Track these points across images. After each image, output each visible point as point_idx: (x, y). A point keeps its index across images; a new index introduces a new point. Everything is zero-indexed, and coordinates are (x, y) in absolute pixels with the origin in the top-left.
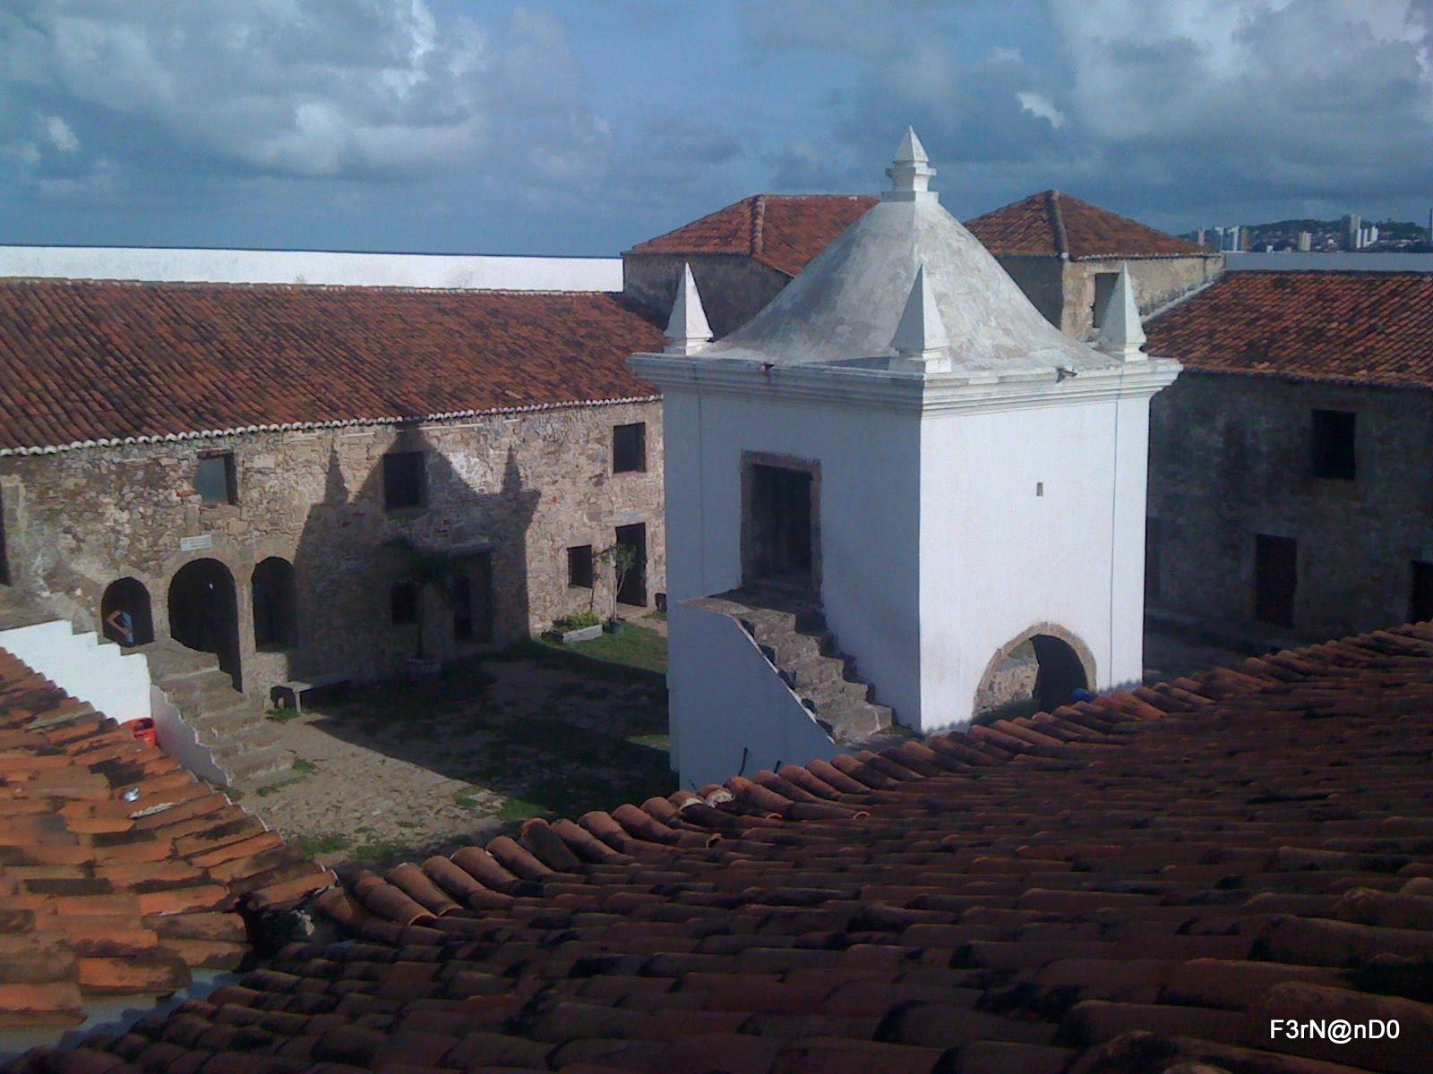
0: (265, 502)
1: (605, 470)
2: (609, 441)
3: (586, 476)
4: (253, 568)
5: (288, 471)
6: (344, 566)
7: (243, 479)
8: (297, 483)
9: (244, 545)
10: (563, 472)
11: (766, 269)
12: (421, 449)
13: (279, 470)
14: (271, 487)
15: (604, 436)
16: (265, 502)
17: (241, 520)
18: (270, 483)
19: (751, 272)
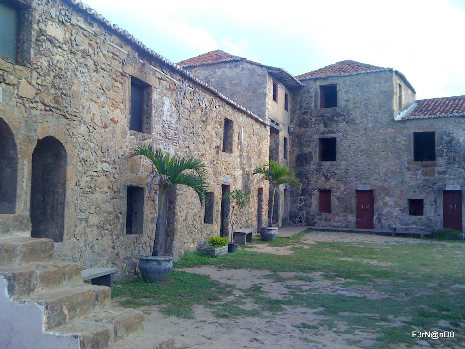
0: (52, 74)
1: (220, 145)
2: (223, 126)
3: (214, 145)
4: (35, 143)
5: (71, 53)
6: (101, 166)
7: (37, 40)
8: (77, 69)
9: (30, 114)
10: (207, 137)
11: (253, 66)
12: (151, 84)
13: (65, 47)
14: (58, 61)
15: (222, 122)
16: (52, 74)
17: (30, 84)
18: (58, 57)
19: (243, 69)
